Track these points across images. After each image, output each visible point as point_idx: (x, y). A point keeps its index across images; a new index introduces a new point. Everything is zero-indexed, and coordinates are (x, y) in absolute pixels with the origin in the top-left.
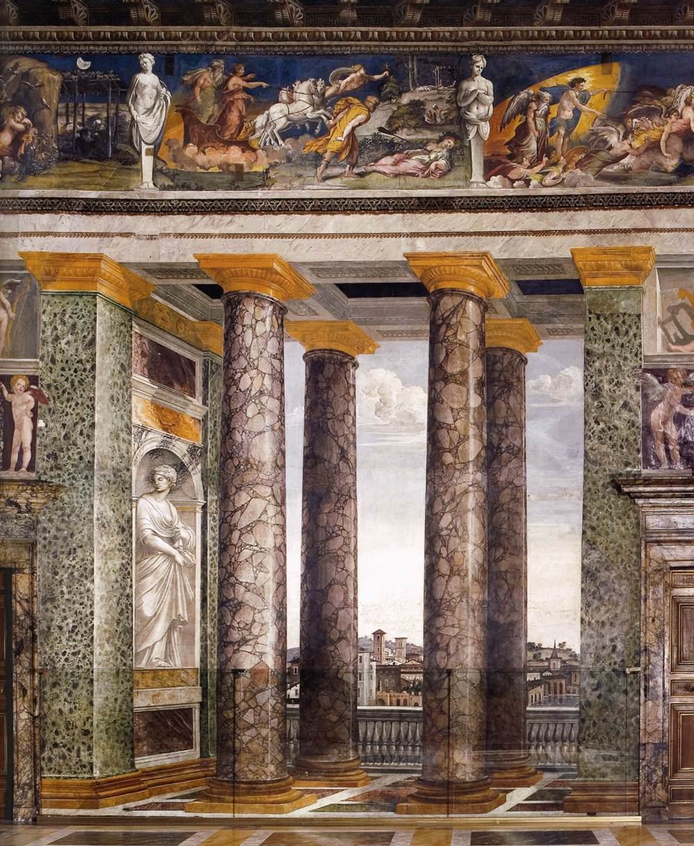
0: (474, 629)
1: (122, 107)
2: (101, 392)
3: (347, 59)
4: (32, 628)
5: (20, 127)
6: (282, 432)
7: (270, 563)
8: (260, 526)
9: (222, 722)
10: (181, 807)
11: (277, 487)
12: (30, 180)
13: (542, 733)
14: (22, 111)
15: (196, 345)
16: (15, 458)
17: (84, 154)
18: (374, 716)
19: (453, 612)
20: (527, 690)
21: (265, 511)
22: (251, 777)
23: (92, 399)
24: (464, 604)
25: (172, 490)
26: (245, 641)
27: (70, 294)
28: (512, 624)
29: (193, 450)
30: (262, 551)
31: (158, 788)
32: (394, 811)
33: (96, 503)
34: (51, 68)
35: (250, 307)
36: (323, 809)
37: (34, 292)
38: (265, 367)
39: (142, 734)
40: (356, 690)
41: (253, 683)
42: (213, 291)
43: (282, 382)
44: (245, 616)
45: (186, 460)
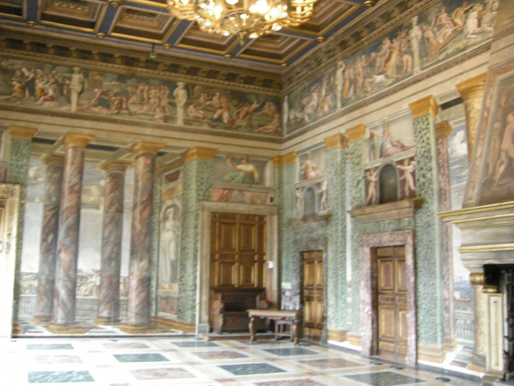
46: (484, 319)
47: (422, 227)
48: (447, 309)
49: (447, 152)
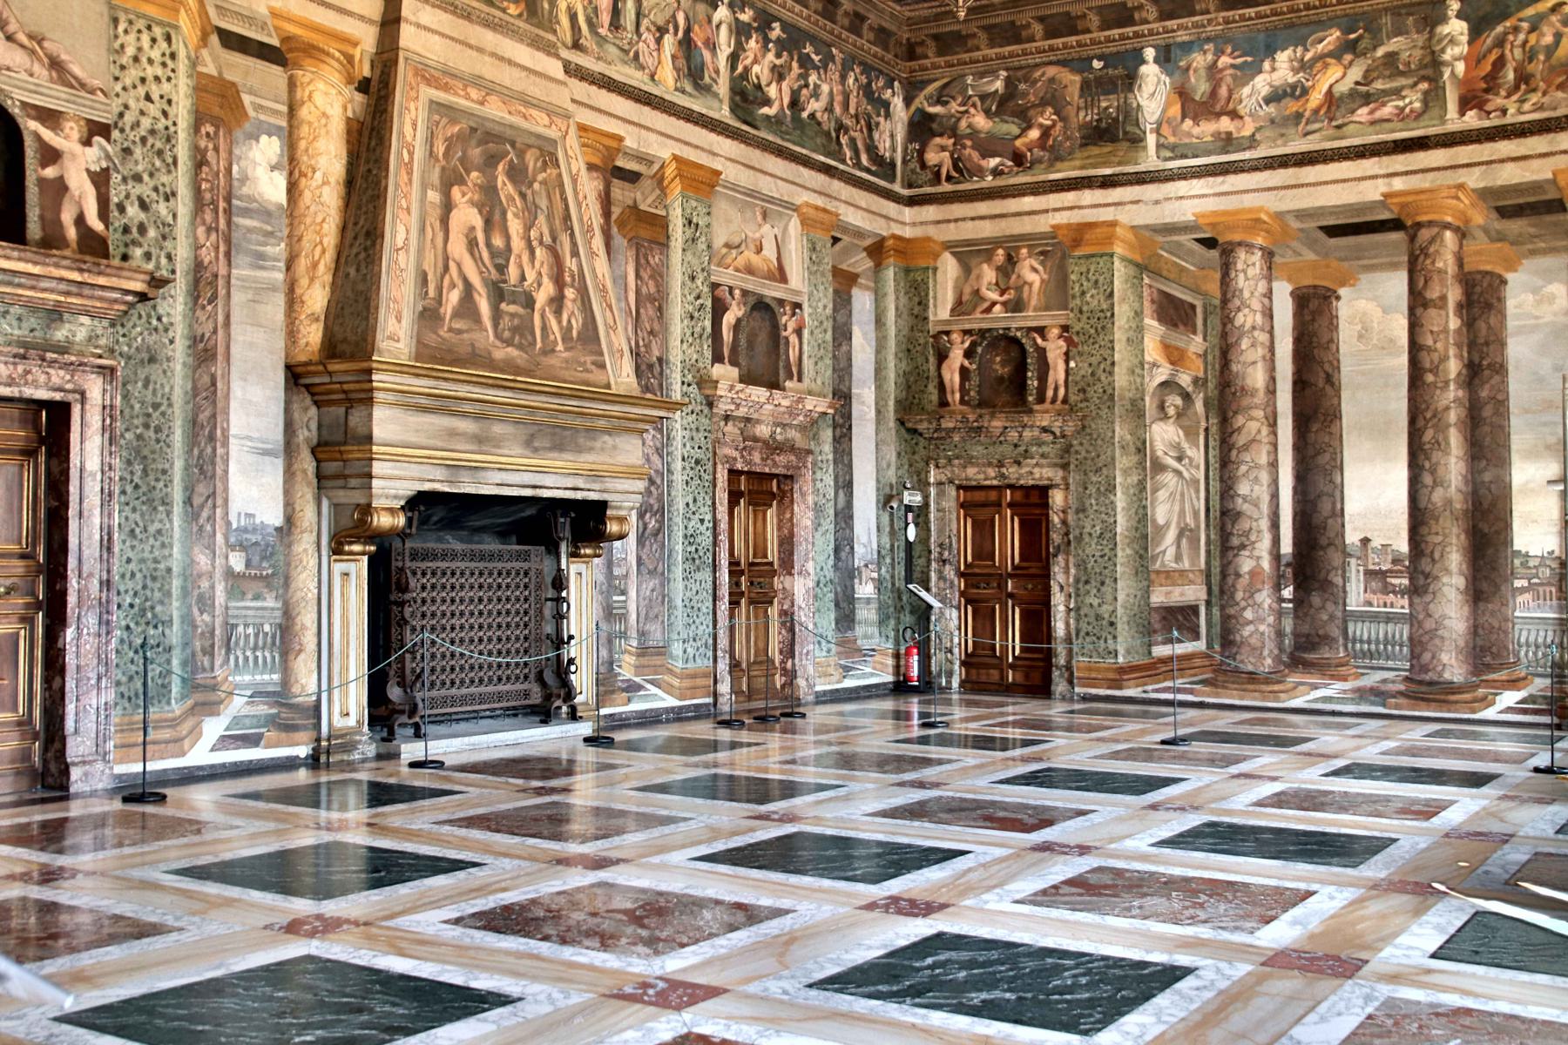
0: (1458, 536)
1: (1130, 96)
2: (1119, 336)
3: (1323, 25)
4: (1067, 534)
5: (1049, 123)
6: (1273, 361)
7: (1265, 477)
8: (1254, 446)
9: (1226, 618)
10: (1191, 692)
11: (1269, 410)
12: (1059, 165)
13: (1532, 639)
14: (1050, 110)
15: (1196, 291)
16: (1050, 393)
17: (1101, 138)
18: (1361, 617)
19: (1437, 520)
20: (1514, 597)
21: (1259, 431)
22: (1250, 668)
23: (1112, 341)
24: (1447, 513)
25: (1179, 415)
26: (1243, 547)
27: (1093, 256)
28: (1497, 533)
29: (1196, 381)
30: (1258, 467)
31: (1170, 675)
32: (1384, 706)
33: (1117, 429)
34: (1073, 71)
35: (1242, 255)
36: (1316, 700)
37: (1064, 257)
38: (1256, 305)
39: (1157, 626)
40: (1345, 592)
41: (1251, 584)
42: (1209, 243)
43: (1271, 317)
44: (1244, 524)
45: (1190, 389)
46: (307, 618)
47: (129, 358)
48: (205, 603)
49: (229, 170)
